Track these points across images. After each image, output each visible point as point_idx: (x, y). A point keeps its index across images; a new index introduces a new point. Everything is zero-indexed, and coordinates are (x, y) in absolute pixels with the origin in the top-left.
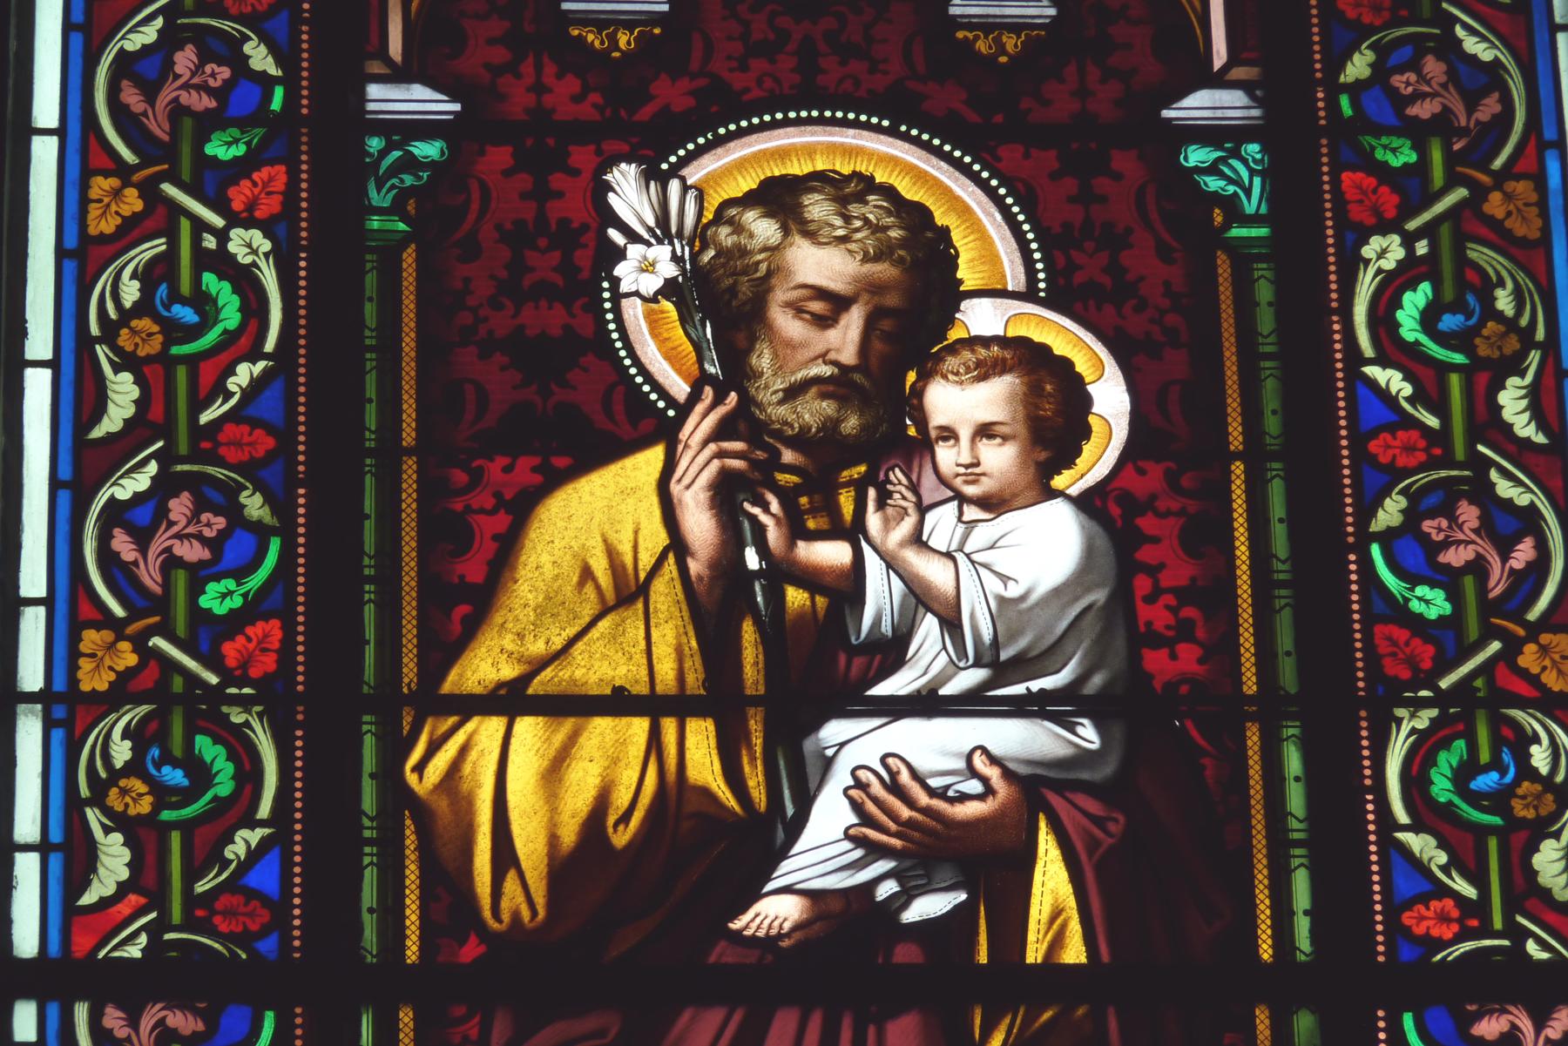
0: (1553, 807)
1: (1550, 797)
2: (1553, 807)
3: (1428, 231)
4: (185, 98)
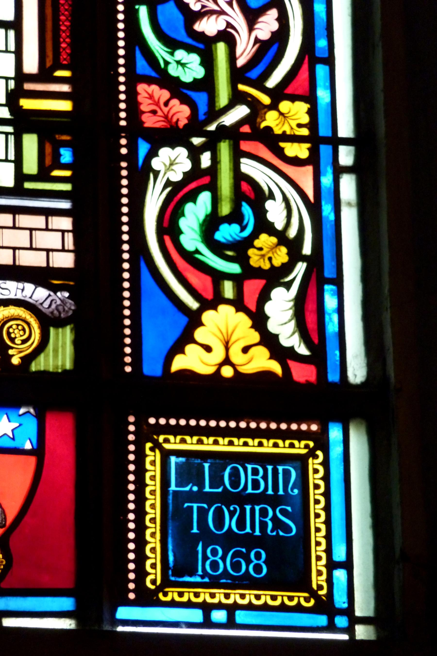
0: (285, 259)
1: (284, 250)
2: (285, 259)
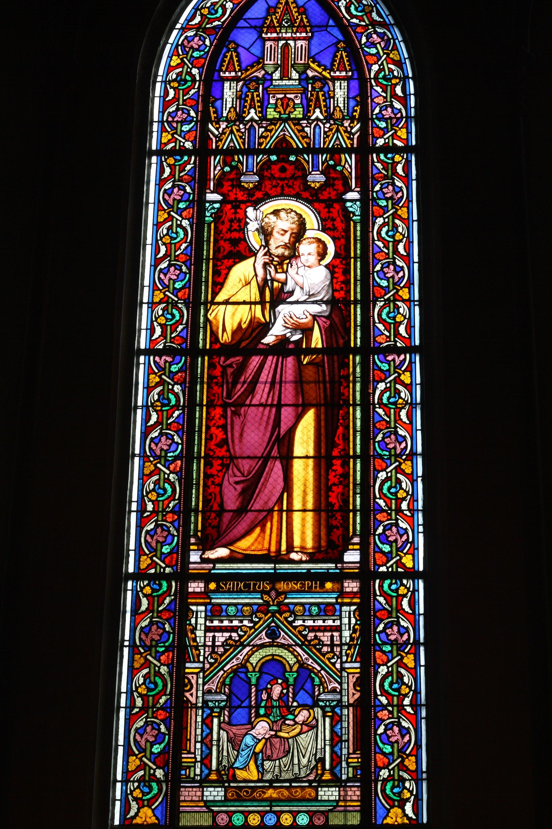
3: (392, 666)
4: (154, 637)
